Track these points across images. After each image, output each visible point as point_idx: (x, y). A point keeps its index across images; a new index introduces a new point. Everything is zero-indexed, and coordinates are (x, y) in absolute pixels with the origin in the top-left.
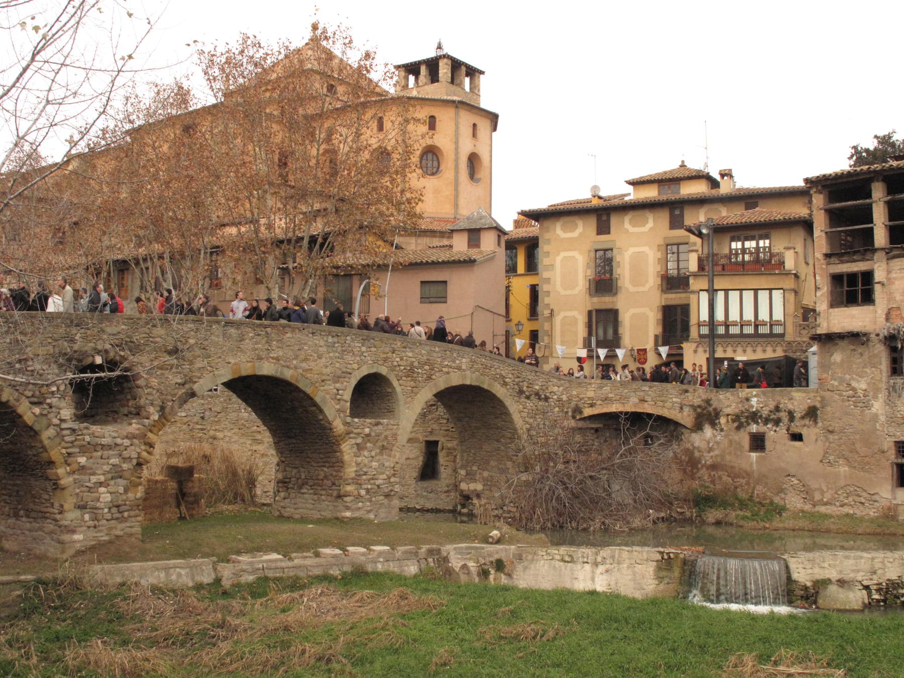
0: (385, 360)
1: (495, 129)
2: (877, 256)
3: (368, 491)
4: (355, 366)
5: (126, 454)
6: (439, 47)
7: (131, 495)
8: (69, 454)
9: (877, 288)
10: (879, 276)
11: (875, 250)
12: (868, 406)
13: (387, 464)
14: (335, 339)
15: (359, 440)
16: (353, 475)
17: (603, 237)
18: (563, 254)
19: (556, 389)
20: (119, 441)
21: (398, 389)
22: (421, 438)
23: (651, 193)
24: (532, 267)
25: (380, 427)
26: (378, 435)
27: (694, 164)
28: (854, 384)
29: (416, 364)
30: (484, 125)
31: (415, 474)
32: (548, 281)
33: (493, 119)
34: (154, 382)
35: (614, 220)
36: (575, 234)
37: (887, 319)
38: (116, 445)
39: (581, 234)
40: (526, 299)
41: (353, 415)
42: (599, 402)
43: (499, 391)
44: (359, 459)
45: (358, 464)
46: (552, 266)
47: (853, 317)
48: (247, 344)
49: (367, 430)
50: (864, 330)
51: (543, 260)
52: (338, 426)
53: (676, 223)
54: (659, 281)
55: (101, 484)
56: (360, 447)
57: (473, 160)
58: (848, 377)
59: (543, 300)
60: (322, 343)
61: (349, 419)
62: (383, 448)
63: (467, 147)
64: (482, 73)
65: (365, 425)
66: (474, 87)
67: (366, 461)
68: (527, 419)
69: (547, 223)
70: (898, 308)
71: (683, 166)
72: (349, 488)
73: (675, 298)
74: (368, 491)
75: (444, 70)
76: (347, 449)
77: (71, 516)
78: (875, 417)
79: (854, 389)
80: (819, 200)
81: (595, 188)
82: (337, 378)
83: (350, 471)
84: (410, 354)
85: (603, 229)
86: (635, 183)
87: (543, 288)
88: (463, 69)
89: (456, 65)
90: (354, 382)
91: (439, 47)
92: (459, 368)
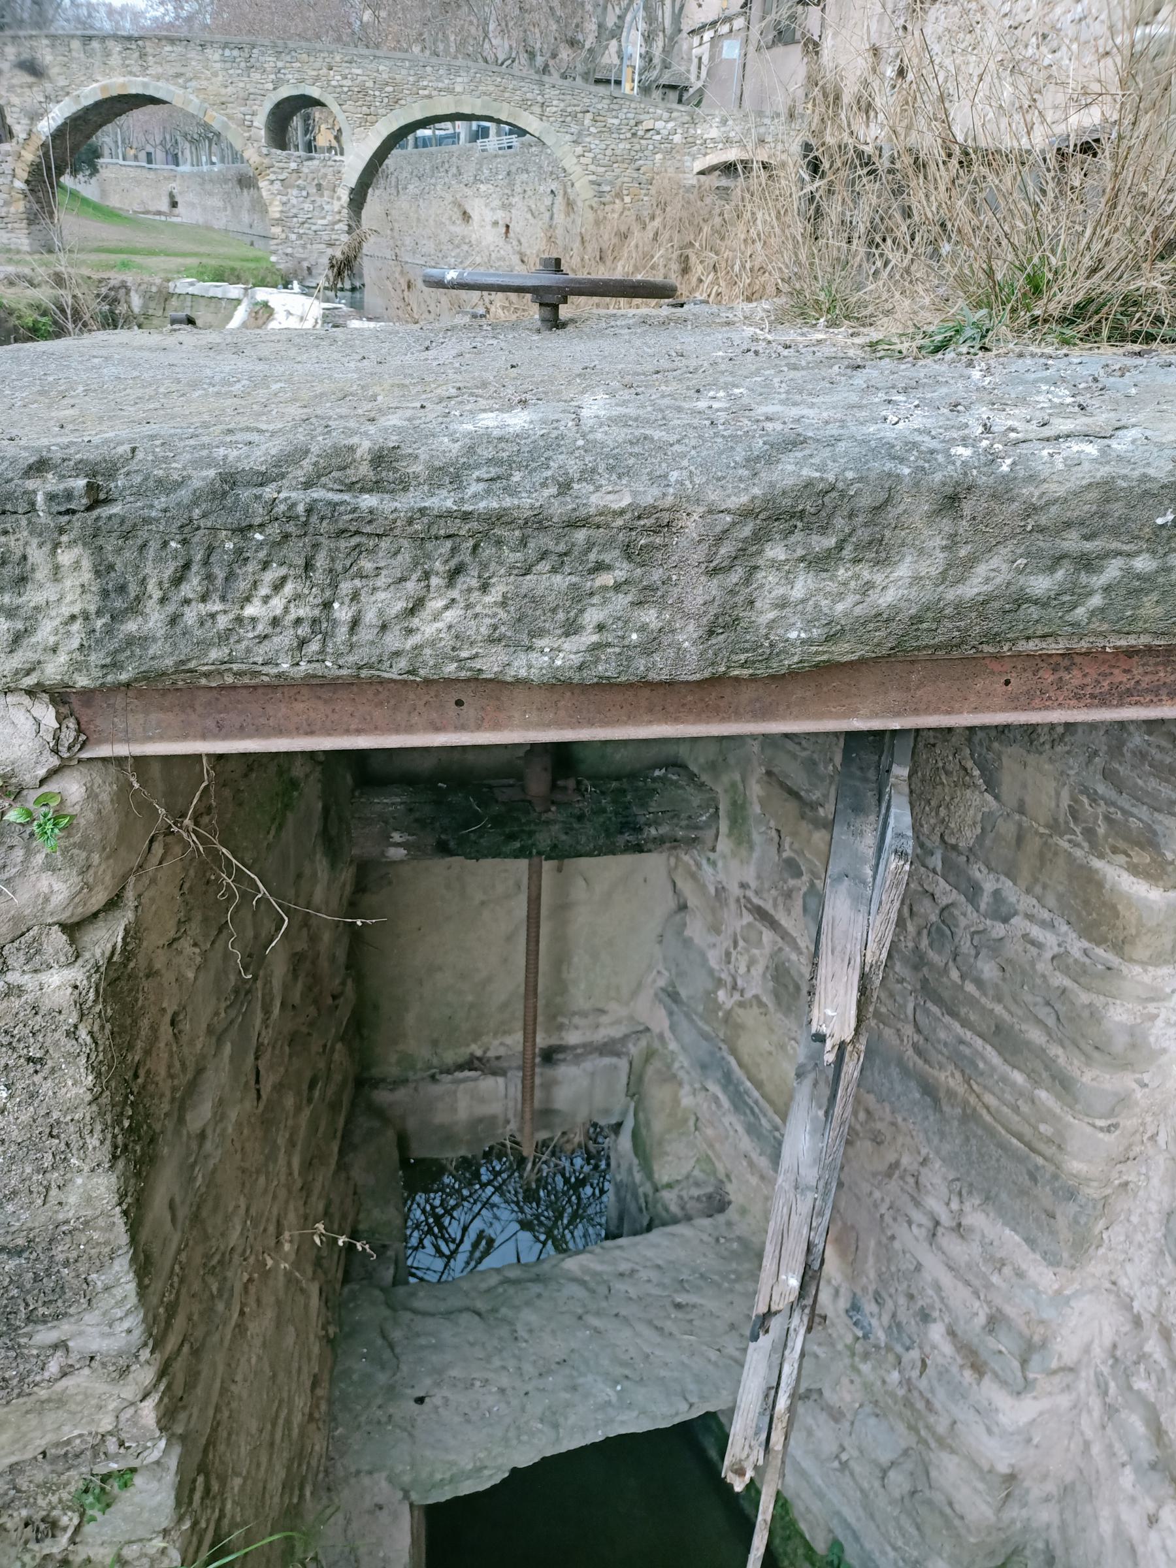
0: (317, 79)
3: (300, 236)
4: (270, 86)
7: (12, 210)
13: (327, 207)
14: (236, 53)
16: (277, 215)
19: (659, 125)
25: (316, 162)
29: (370, 84)
34: (15, 100)
42: (720, 146)
44: (284, 199)
48: (115, 60)
49: (293, 165)
60: (217, 57)
61: (265, 151)
67: (294, 201)
68: (592, 168)
72: (276, 230)
74: (300, 236)
83: (275, 210)
84: (359, 71)
90: (268, 106)
92: (450, 91)
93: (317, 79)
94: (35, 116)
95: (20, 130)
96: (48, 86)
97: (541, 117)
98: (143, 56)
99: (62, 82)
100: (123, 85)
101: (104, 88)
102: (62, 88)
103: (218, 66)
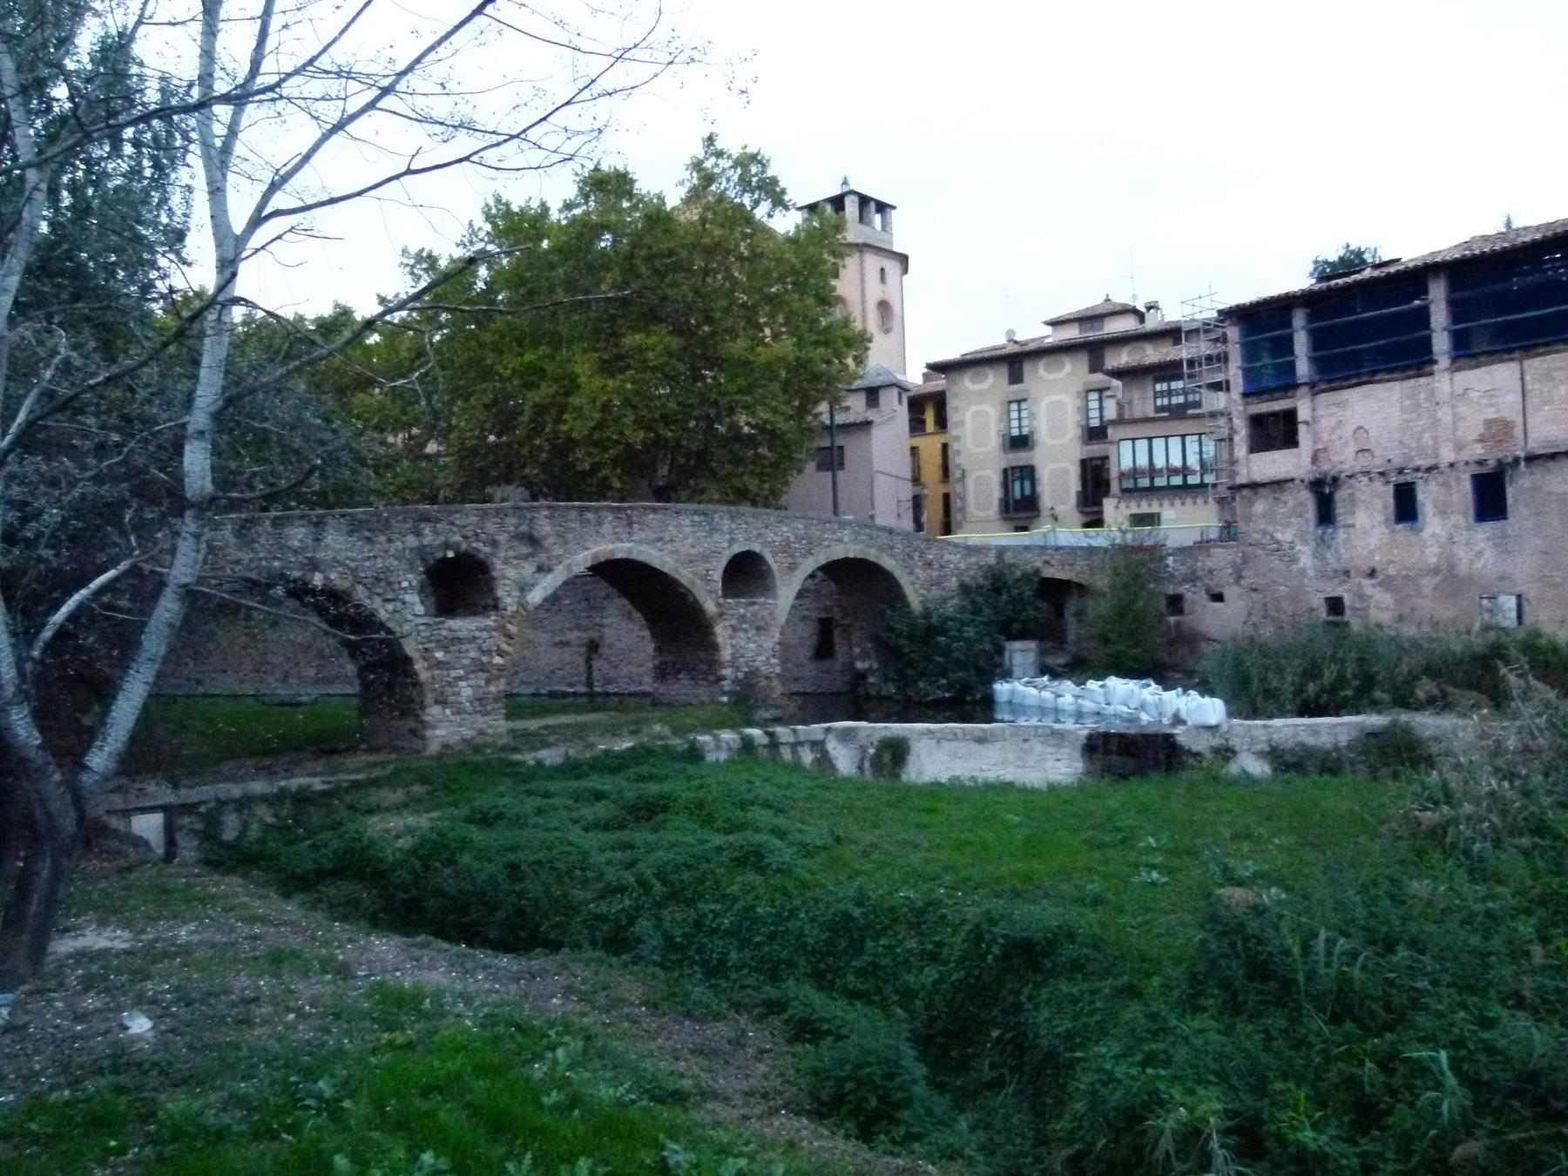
0: (760, 535)
1: (905, 271)
2: (1304, 390)
5: (485, 647)
6: (845, 182)
7: (492, 689)
8: (426, 650)
9: (1302, 429)
10: (1303, 413)
11: (1296, 386)
12: (1294, 560)
15: (734, 622)
17: (1016, 387)
18: (974, 408)
20: (477, 634)
21: (774, 567)
22: (814, 615)
23: (1072, 333)
24: (942, 423)
26: (754, 615)
27: (1121, 298)
28: (1279, 536)
30: (892, 267)
31: (810, 654)
32: (957, 439)
33: (903, 260)
35: (1027, 368)
36: (985, 385)
37: (1315, 459)
38: (475, 638)
39: (992, 386)
40: (938, 459)
41: (725, 596)
43: (887, 563)
45: (733, 646)
46: (961, 424)
47: (1275, 461)
48: (607, 528)
49: (742, 611)
50: (1288, 476)
51: (952, 417)
52: (710, 607)
53: (1096, 367)
54: (1079, 432)
55: (460, 678)
56: (735, 629)
57: (884, 306)
58: (1271, 528)
59: (955, 460)
60: (687, 522)
61: (721, 601)
62: (759, 628)
63: (874, 293)
64: (893, 207)
65: (738, 607)
66: (885, 226)
67: (742, 643)
69: (954, 376)
70: (1325, 450)
71: (1107, 300)
73: (1096, 449)
75: (851, 207)
76: (721, 632)
77: (433, 712)
78: (1303, 572)
79: (1278, 542)
80: (1233, 333)
81: (1011, 332)
82: (706, 558)
83: (726, 654)
85: (1016, 378)
86: (1055, 324)
87: (954, 446)
88: (873, 205)
89: (864, 201)
90: (724, 562)
91: (845, 182)
92: (840, 541)
93: (760, 535)
94: (524, 588)
95: (509, 602)
96: (542, 557)
97: (893, 556)
98: (630, 524)
99: (558, 551)
100: (612, 552)
101: (595, 556)
102: (557, 557)
103: (688, 530)
